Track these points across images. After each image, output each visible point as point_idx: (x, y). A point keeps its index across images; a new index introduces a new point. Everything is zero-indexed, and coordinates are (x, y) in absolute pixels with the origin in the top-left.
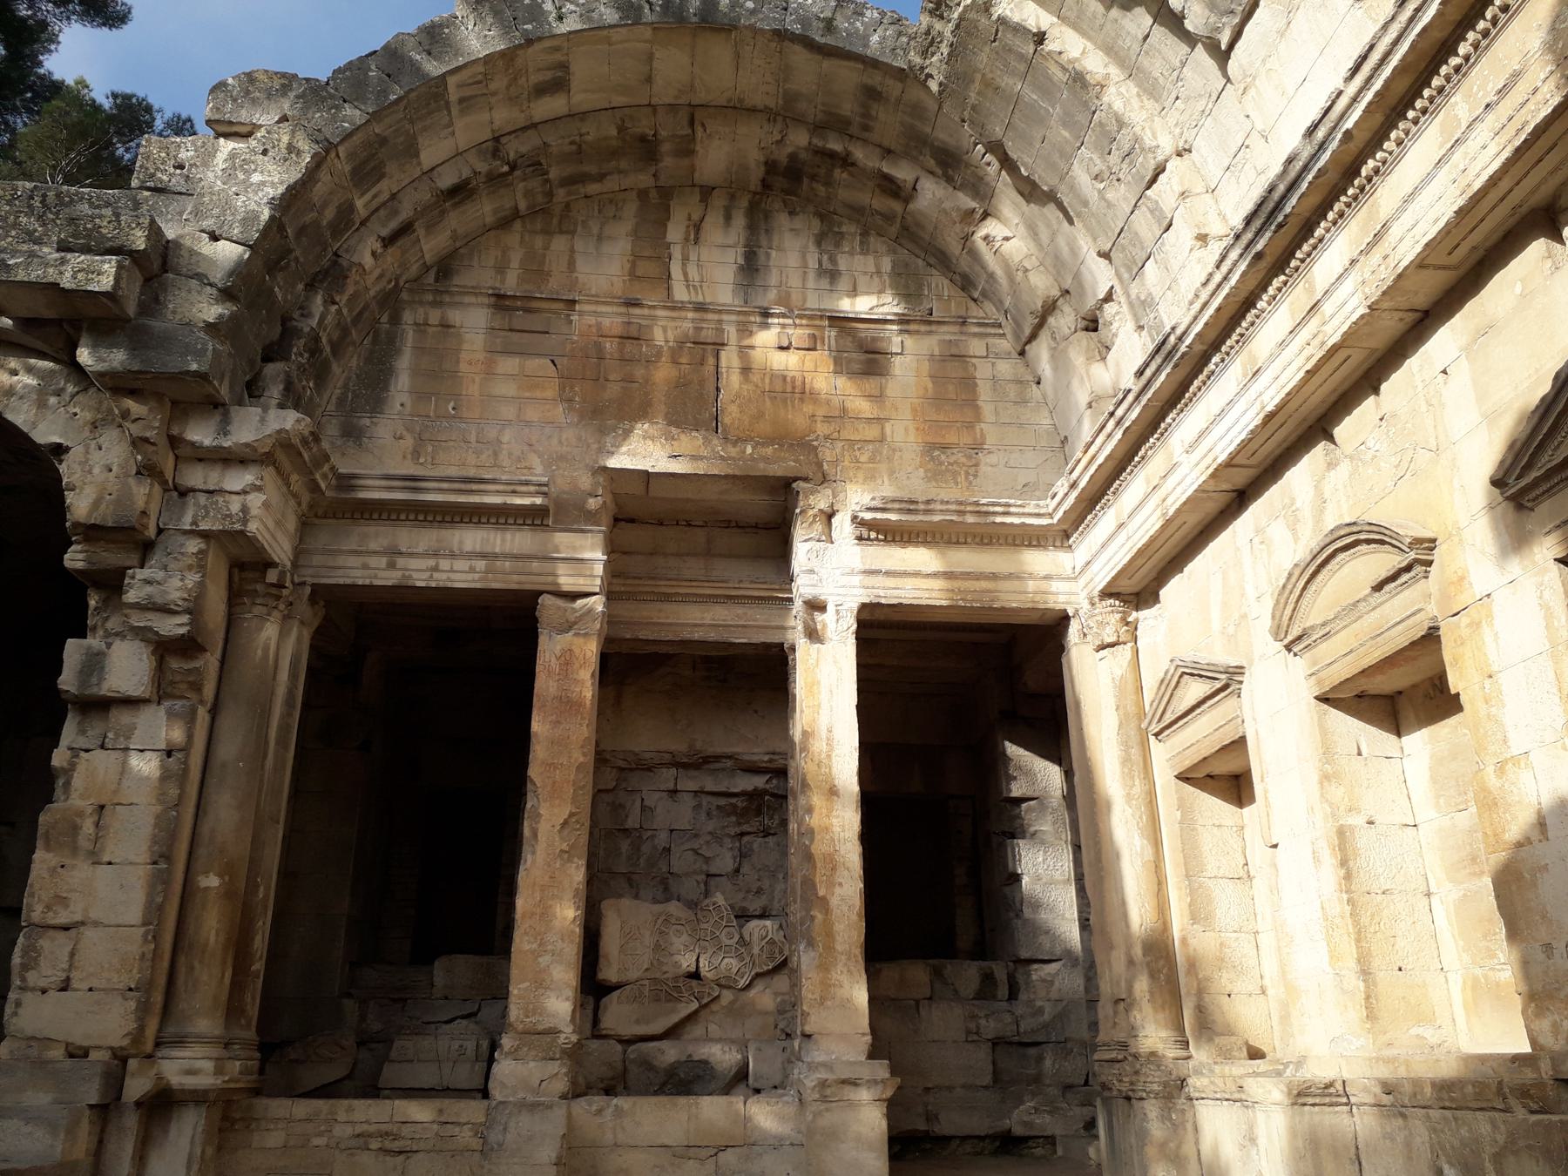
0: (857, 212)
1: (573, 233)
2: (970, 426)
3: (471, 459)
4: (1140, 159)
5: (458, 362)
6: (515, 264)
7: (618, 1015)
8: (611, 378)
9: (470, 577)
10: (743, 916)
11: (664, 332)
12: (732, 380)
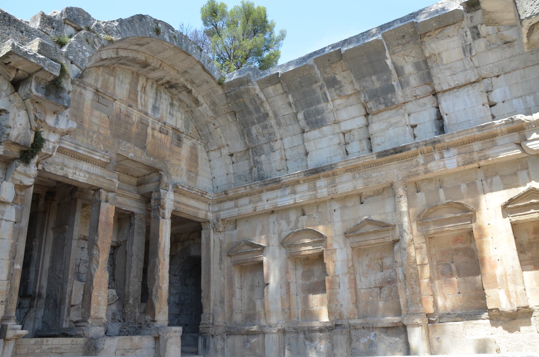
0: (180, 100)
1: (115, 77)
2: (196, 168)
3: (85, 140)
4: (273, 136)
5: (83, 107)
6: (100, 81)
8: (122, 126)
9: (84, 179)
11: (135, 116)
12: (150, 139)
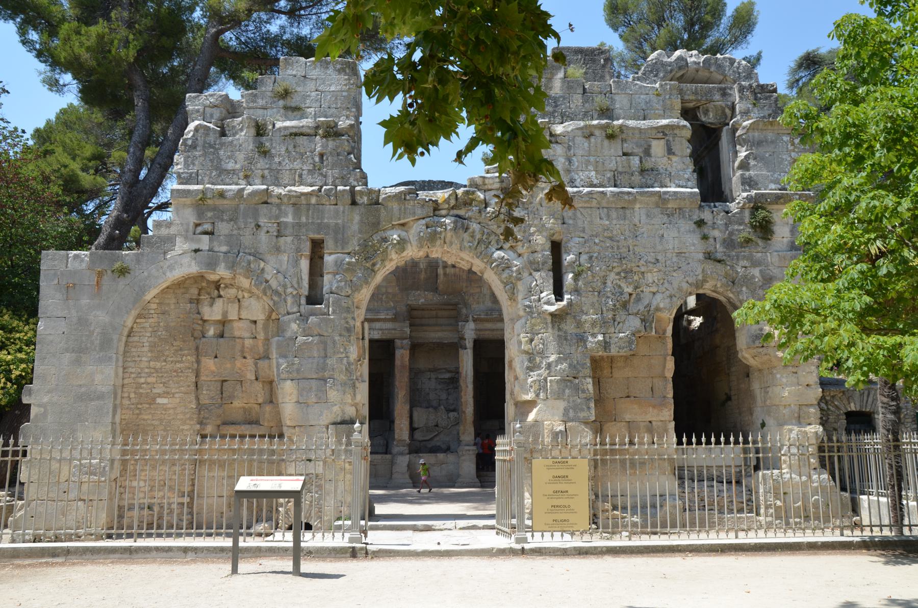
3: (376, 304)
7: (418, 436)
10: (449, 411)
12: (441, 278)
